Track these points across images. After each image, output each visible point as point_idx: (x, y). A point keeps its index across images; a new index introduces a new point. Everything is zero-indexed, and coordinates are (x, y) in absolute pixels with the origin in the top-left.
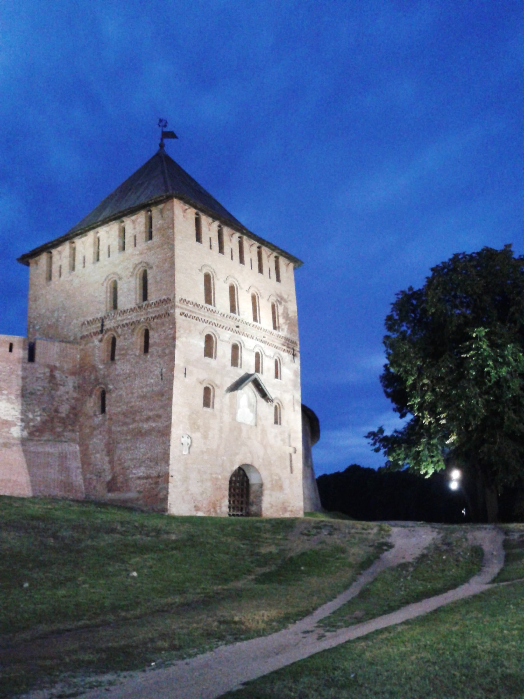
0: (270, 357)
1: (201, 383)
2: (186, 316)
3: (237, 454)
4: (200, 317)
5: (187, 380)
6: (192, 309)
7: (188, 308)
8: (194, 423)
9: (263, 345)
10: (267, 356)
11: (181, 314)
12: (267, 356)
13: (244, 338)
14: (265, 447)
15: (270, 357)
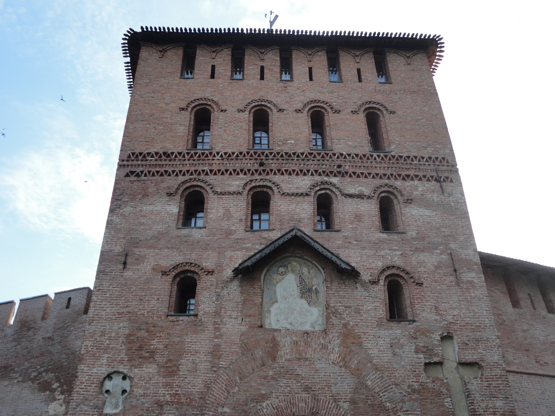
0: (360, 196)
1: (164, 273)
2: (138, 175)
3: (264, 397)
4: (170, 170)
5: (128, 274)
6: (156, 163)
7: (148, 163)
8: (140, 348)
9: (334, 180)
10: (351, 196)
11: (127, 175)
12: (351, 196)
13: (277, 178)
14: (357, 373)
15: (360, 196)
